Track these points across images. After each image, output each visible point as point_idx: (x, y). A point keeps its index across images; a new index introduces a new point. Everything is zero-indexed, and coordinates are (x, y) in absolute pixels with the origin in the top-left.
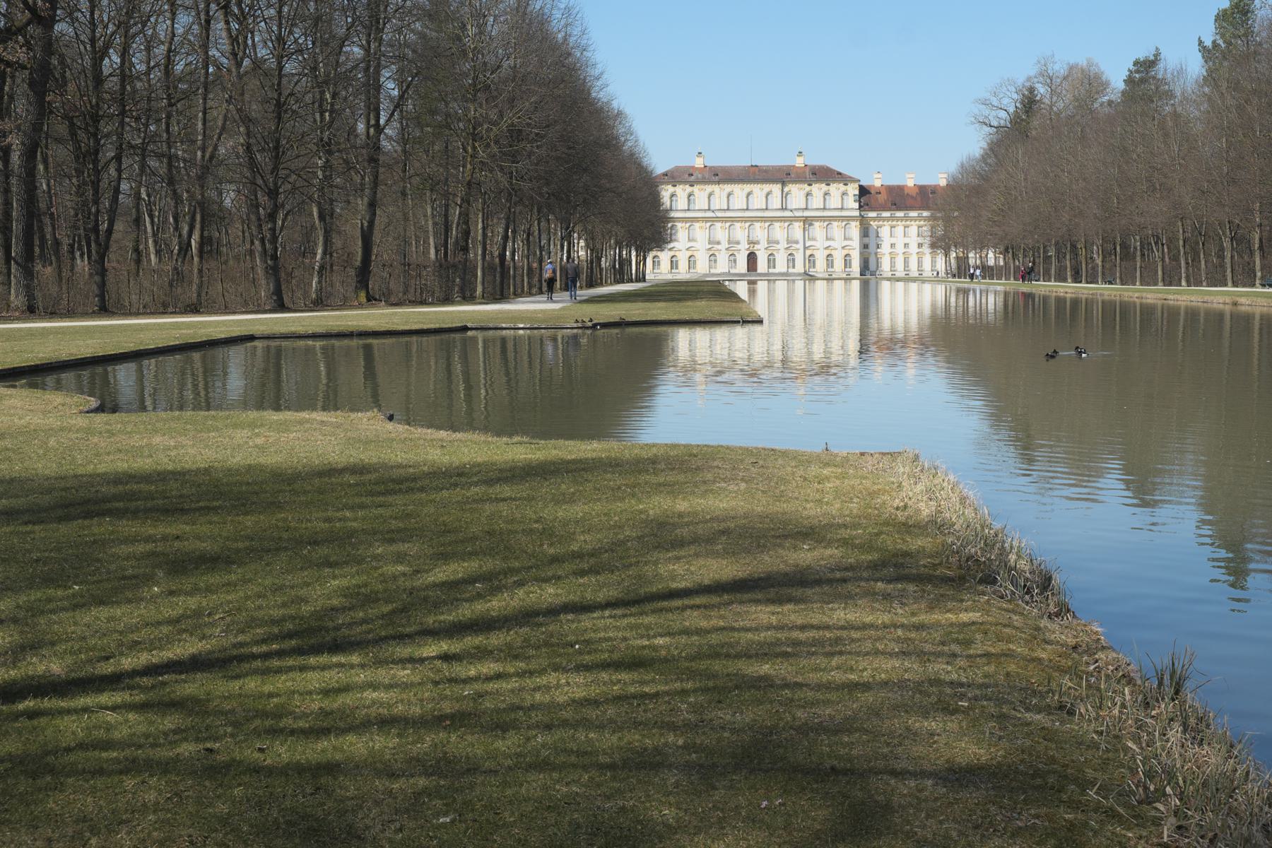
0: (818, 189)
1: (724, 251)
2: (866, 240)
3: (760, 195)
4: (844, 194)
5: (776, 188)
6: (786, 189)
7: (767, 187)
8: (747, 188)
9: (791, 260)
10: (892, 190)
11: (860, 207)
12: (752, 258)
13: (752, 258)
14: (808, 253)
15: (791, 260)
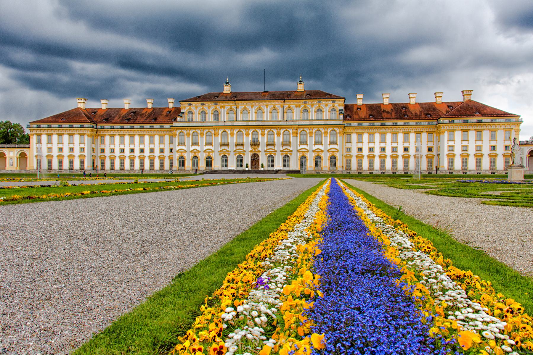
0: (313, 105)
1: (232, 153)
2: (348, 145)
3: (269, 112)
4: (333, 110)
5: (278, 104)
6: (286, 106)
7: (272, 104)
8: (257, 104)
9: (286, 161)
10: (370, 107)
11: (345, 119)
12: (255, 158)
13: (255, 158)
14: (299, 155)
15: (286, 161)
